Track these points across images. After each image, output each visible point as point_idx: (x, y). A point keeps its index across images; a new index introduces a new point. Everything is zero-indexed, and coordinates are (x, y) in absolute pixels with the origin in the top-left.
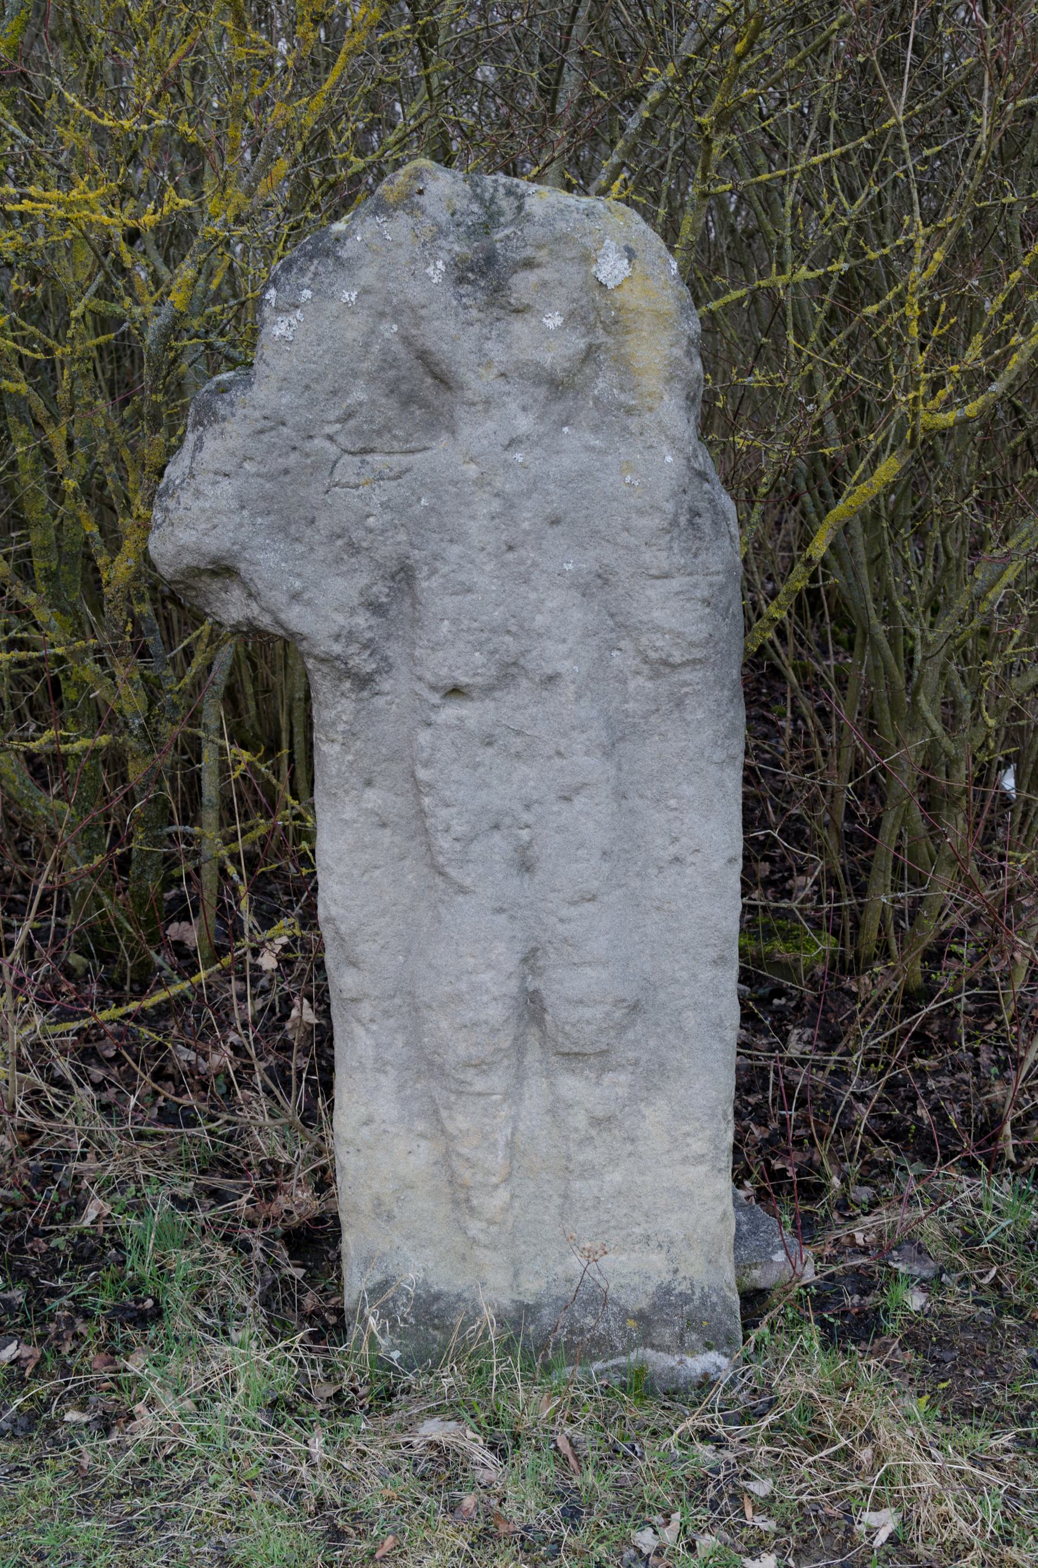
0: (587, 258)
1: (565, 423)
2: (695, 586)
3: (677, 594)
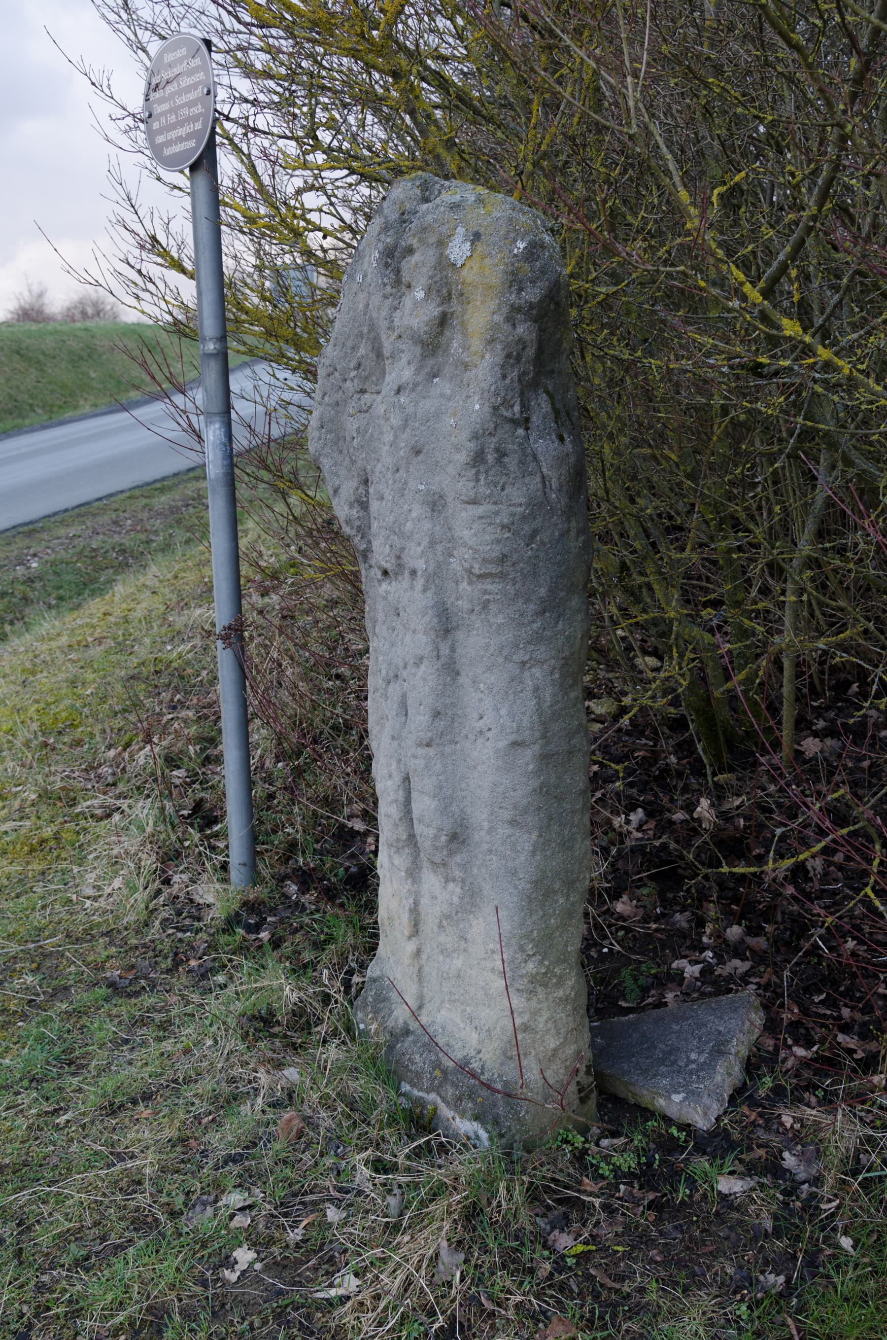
0: (442, 244)
1: (435, 376)
2: (497, 513)
3: (481, 518)
